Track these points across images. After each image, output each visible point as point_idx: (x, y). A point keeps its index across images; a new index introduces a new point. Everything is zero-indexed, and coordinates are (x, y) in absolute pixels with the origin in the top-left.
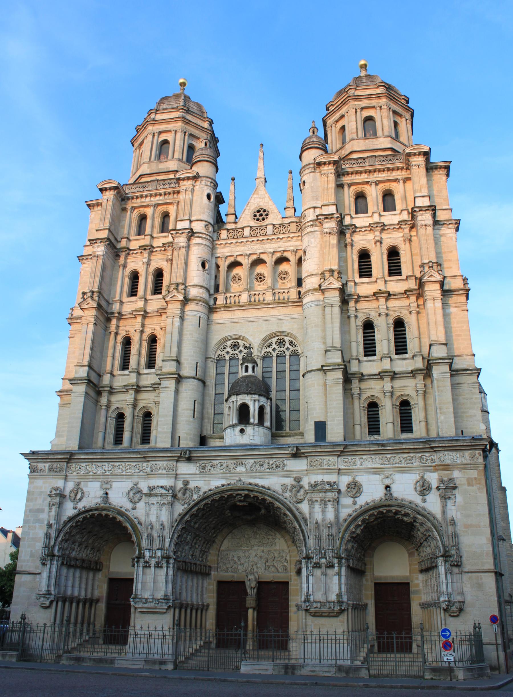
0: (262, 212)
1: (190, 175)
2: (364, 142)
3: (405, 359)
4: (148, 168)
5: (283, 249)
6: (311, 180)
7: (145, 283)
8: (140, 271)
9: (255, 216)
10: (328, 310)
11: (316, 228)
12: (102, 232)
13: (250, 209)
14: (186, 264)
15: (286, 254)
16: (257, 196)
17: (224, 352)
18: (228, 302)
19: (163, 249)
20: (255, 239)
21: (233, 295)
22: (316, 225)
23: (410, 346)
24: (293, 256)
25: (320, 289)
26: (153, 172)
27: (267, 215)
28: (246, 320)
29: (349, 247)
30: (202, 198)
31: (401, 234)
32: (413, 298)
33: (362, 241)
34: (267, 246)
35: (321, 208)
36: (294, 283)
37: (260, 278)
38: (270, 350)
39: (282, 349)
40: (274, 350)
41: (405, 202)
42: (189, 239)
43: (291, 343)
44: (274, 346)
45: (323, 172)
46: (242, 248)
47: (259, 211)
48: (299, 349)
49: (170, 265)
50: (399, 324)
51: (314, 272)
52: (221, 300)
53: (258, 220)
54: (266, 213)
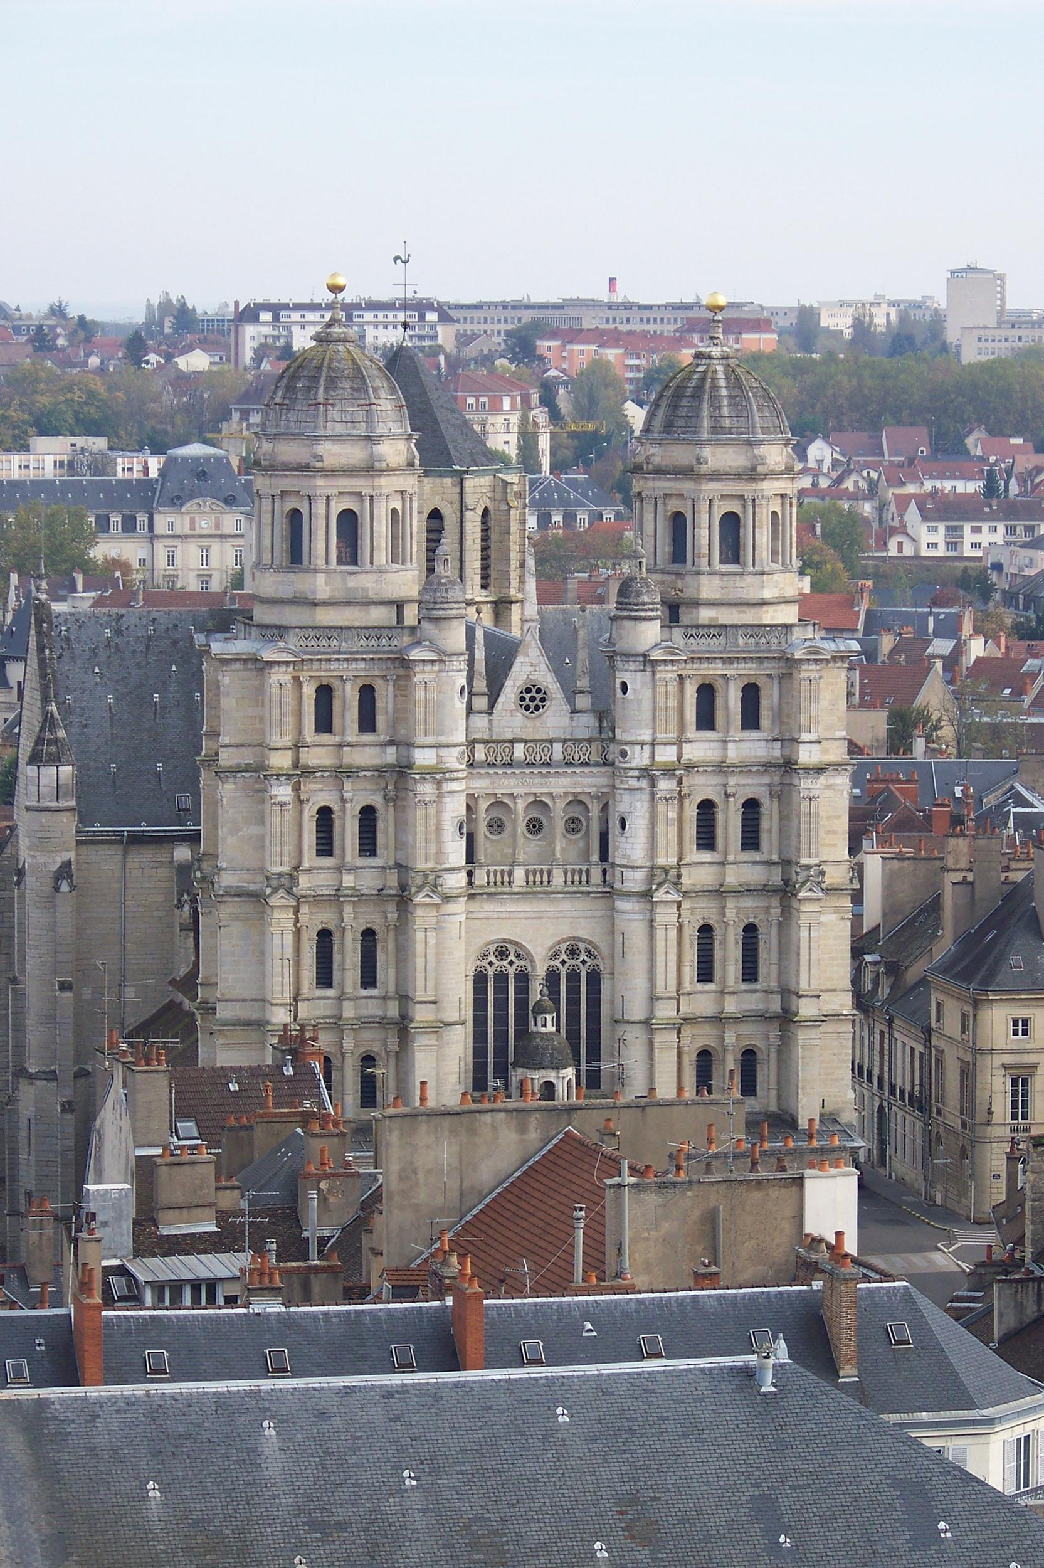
0: (534, 694)
1: (433, 656)
2: (721, 580)
3: (755, 991)
4: (326, 584)
5: (578, 790)
6: (638, 687)
7: (348, 832)
9: (523, 699)
10: (660, 934)
11: (644, 783)
12: (280, 752)
13: (514, 685)
14: (439, 829)
15: (581, 798)
16: (527, 659)
17: (485, 963)
18: (492, 879)
19: (376, 773)
20: (536, 771)
21: (499, 868)
22: (644, 777)
23: (762, 971)
24: (595, 804)
25: (647, 895)
26: (339, 595)
27: (543, 700)
28: (522, 915)
29: (687, 801)
30: (452, 699)
31: (766, 780)
32: (775, 902)
33: (704, 787)
35: (653, 744)
36: (595, 857)
37: (534, 826)
38: (557, 963)
39: (574, 962)
40: (563, 962)
41: (778, 723)
42: (439, 783)
44: (564, 957)
45: (658, 676)
46: (512, 781)
47: (528, 690)
49: (391, 809)
51: (639, 863)
52: (480, 877)
53: (527, 708)
54: (541, 695)
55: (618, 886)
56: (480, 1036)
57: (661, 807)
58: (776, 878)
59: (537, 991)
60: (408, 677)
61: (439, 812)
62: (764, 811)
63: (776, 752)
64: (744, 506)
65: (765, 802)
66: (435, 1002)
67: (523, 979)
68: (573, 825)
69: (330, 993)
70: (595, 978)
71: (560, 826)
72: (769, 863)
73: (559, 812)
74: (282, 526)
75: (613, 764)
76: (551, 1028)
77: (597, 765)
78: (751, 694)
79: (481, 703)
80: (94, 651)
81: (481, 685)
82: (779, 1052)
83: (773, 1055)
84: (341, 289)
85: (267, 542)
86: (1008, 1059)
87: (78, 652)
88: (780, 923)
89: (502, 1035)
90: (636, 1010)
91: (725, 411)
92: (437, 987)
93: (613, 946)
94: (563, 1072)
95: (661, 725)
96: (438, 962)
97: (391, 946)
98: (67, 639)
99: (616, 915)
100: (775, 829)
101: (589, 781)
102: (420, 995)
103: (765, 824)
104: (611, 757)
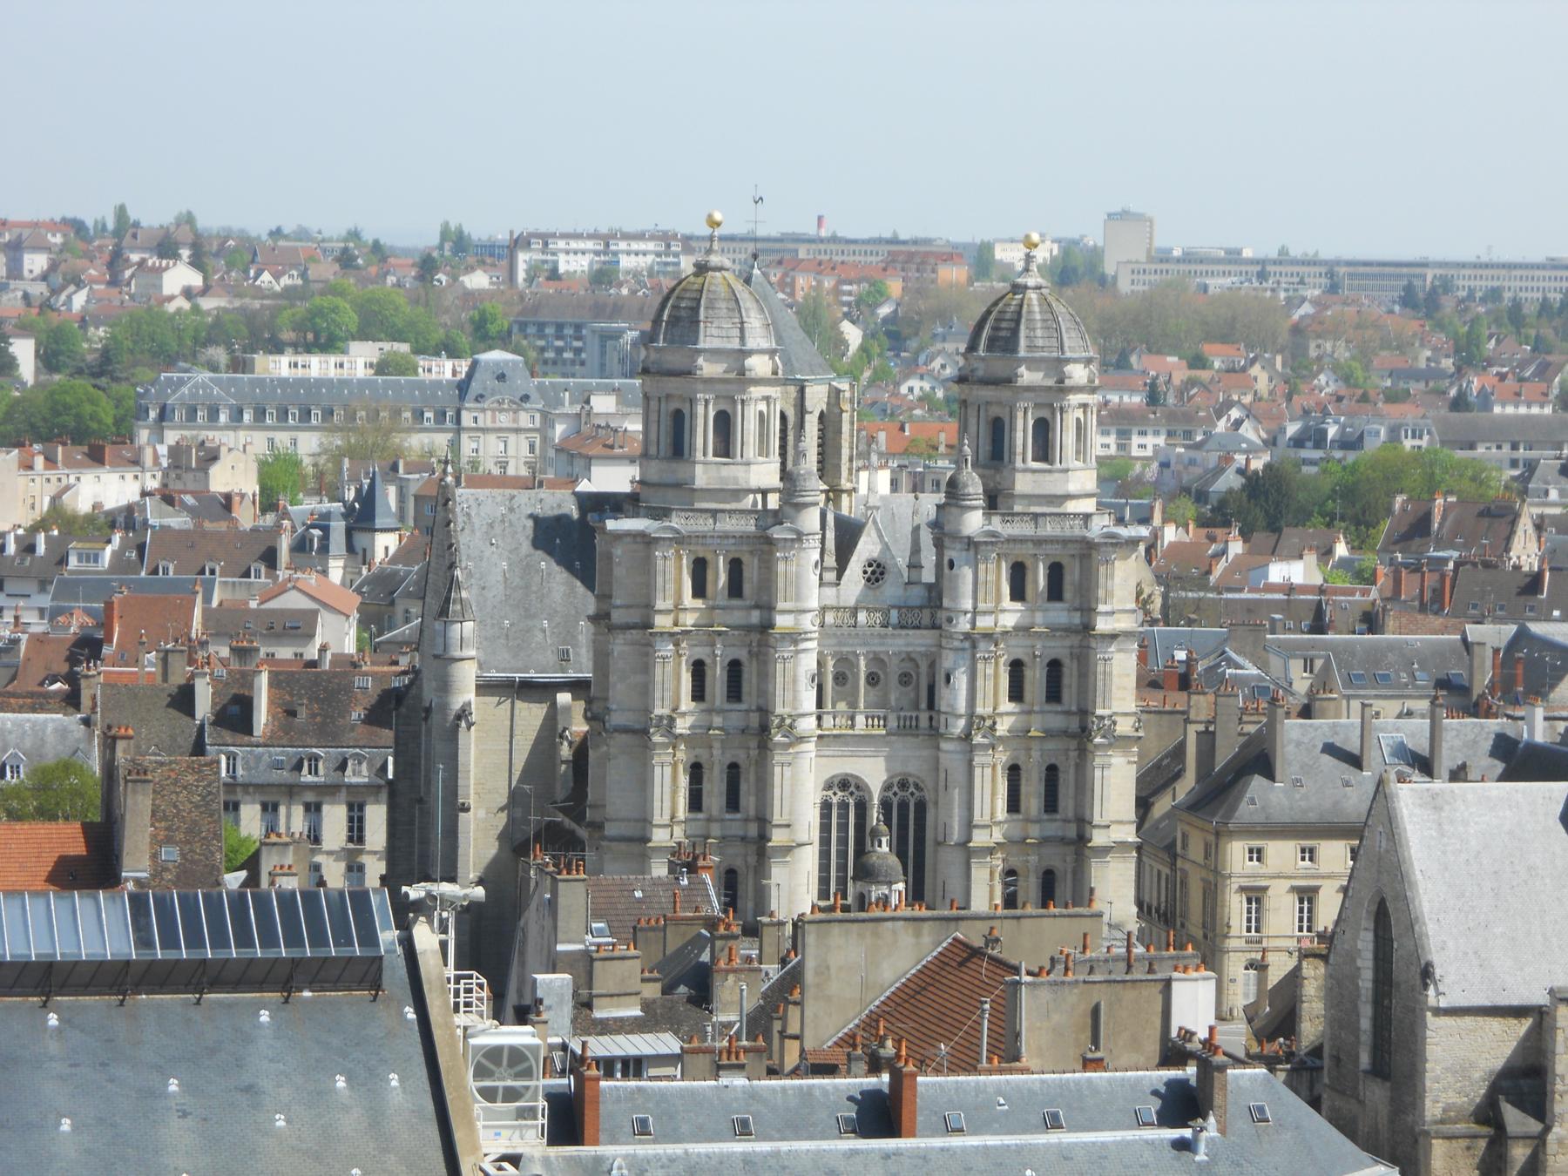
8: (708, 661)
10: (978, 772)
11: (967, 644)
14: (795, 681)
27: (882, 573)
31: (1067, 643)
32: (1073, 744)
34: (890, 641)
36: (923, 705)
38: (890, 794)
43: (917, 786)
44: (895, 789)
48: (929, 796)
49: (754, 663)
50: (1052, 772)
55: (942, 730)
56: (825, 855)
57: (980, 666)
58: (1074, 724)
59: (875, 815)
60: (771, 553)
61: (796, 666)
62: (1066, 671)
63: (1077, 619)
64: (1053, 414)
65: (1066, 661)
66: (788, 826)
67: (862, 808)
68: (905, 679)
69: (700, 816)
70: (921, 807)
71: (894, 680)
72: (1068, 713)
73: (894, 668)
74: (667, 423)
75: (940, 628)
76: (885, 848)
77: (926, 628)
78: (1056, 573)
79: (830, 576)
80: (491, 525)
81: (831, 561)
82: (1075, 873)
83: (1069, 876)
84: (718, 224)
85: (653, 436)
86: (1245, 882)
87: (477, 526)
88: (1077, 765)
89: (843, 854)
90: (956, 835)
91: (1039, 333)
92: (790, 814)
93: (937, 784)
94: (894, 887)
95: (981, 596)
96: (792, 791)
97: (752, 777)
98: (468, 515)
99: (942, 755)
100: (1074, 686)
101: (919, 641)
102: (777, 819)
103: (1066, 681)
104: (938, 622)
